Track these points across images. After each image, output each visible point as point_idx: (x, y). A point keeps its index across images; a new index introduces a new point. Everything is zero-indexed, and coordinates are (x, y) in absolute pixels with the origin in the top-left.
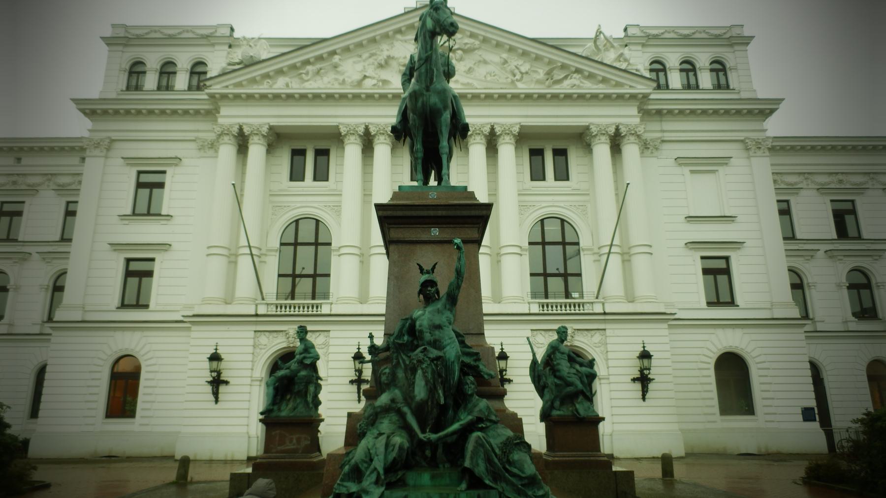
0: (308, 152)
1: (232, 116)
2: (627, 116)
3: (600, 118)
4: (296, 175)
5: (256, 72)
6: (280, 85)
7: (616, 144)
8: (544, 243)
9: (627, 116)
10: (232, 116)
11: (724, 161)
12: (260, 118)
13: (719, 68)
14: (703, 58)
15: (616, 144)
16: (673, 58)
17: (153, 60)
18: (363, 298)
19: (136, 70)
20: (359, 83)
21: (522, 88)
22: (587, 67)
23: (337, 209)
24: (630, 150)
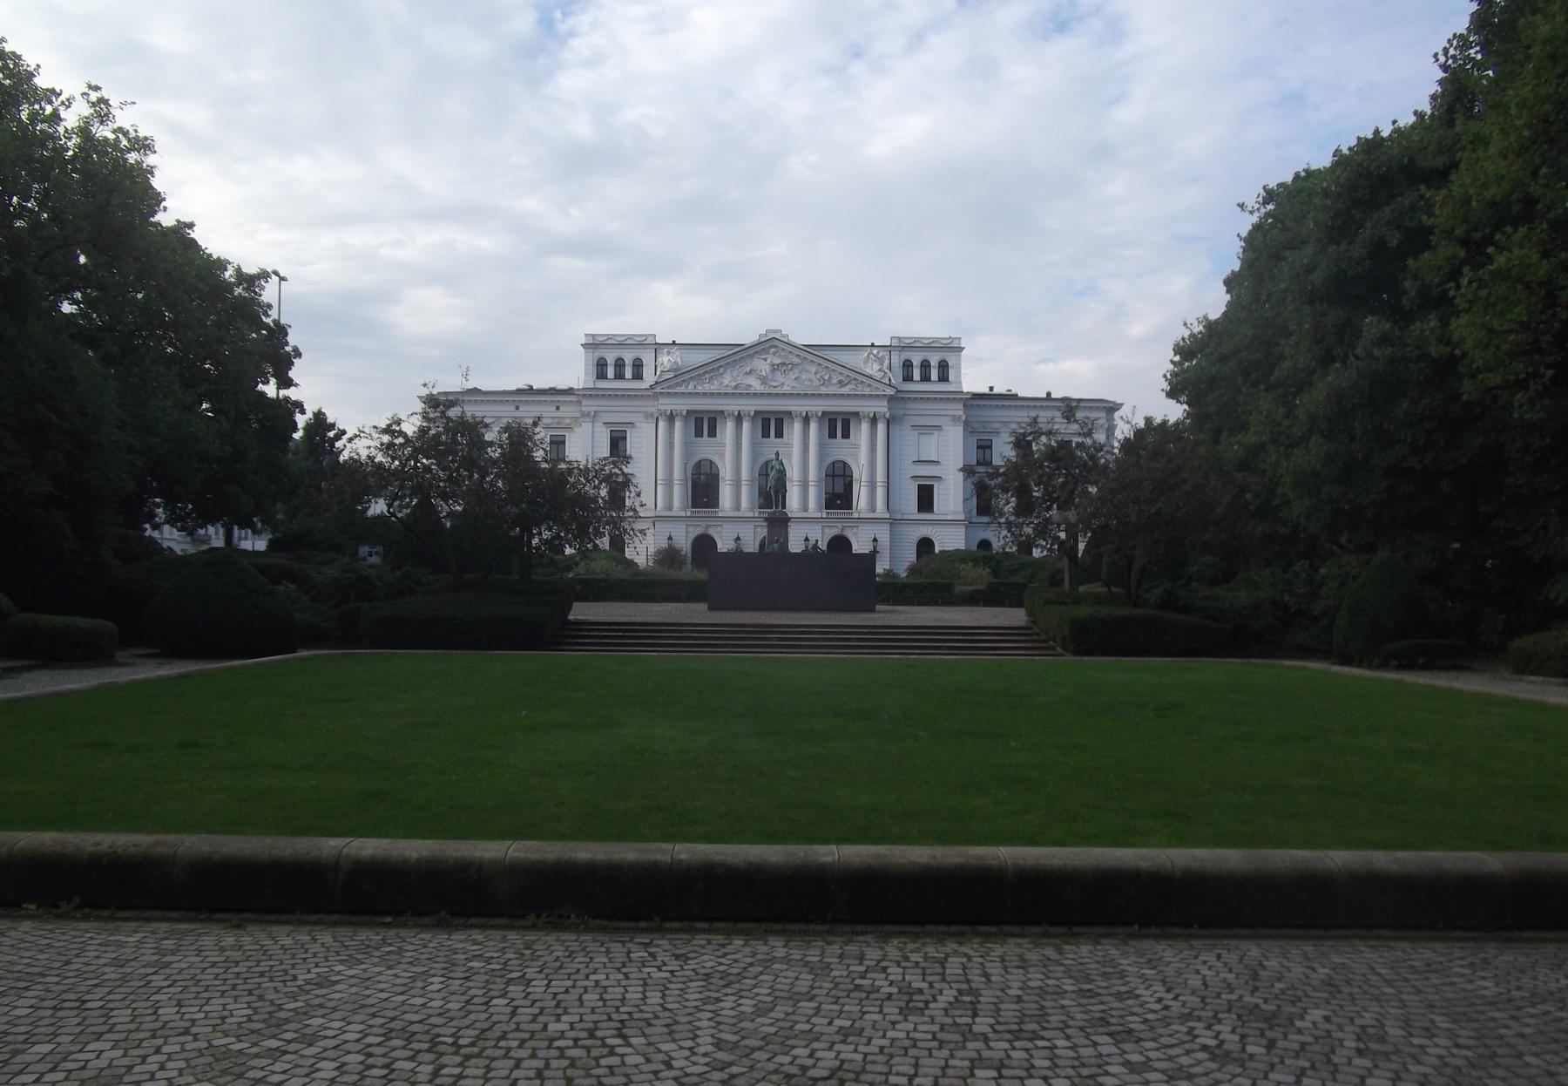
0: (704, 424)
1: (667, 405)
2: (882, 408)
3: (868, 407)
4: (699, 434)
5: (679, 380)
6: (690, 388)
7: (874, 421)
8: (833, 476)
9: (882, 408)
10: (667, 405)
11: (938, 427)
12: (682, 405)
13: (944, 366)
14: (934, 360)
15: (874, 421)
16: (916, 360)
17: (610, 357)
18: (738, 508)
19: (601, 365)
20: (736, 387)
21: (824, 390)
22: (861, 378)
23: (722, 456)
24: (881, 427)
